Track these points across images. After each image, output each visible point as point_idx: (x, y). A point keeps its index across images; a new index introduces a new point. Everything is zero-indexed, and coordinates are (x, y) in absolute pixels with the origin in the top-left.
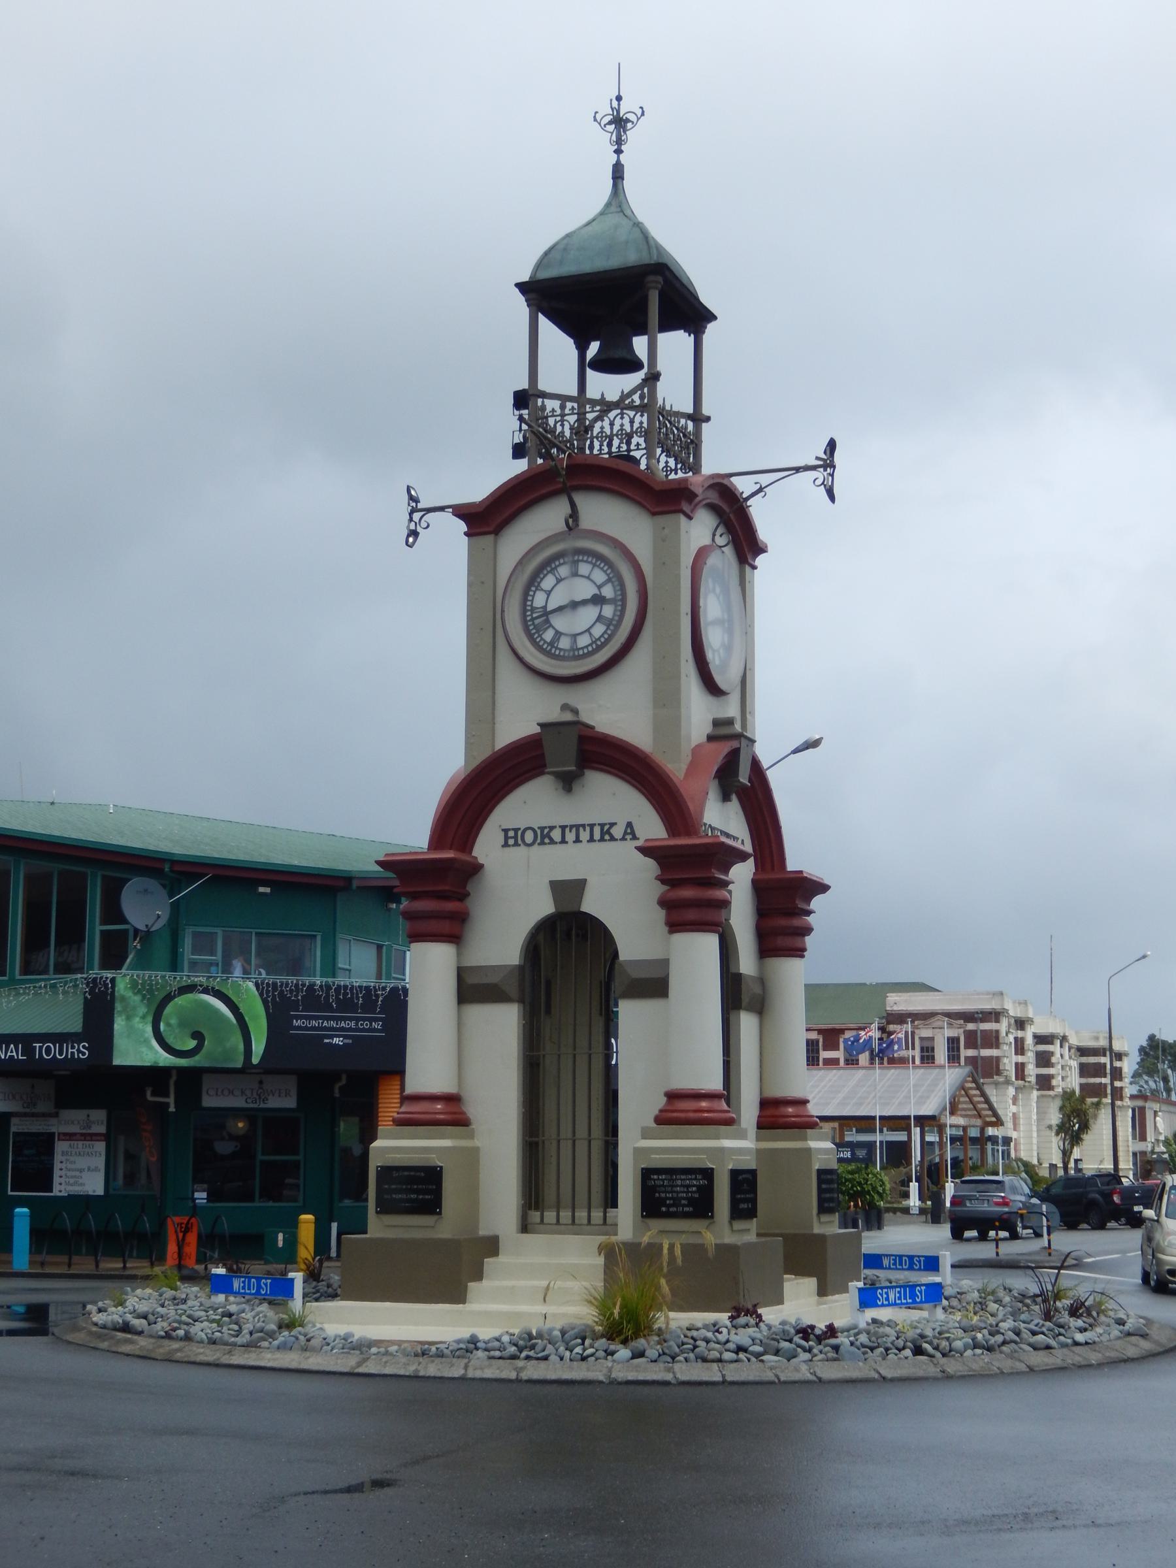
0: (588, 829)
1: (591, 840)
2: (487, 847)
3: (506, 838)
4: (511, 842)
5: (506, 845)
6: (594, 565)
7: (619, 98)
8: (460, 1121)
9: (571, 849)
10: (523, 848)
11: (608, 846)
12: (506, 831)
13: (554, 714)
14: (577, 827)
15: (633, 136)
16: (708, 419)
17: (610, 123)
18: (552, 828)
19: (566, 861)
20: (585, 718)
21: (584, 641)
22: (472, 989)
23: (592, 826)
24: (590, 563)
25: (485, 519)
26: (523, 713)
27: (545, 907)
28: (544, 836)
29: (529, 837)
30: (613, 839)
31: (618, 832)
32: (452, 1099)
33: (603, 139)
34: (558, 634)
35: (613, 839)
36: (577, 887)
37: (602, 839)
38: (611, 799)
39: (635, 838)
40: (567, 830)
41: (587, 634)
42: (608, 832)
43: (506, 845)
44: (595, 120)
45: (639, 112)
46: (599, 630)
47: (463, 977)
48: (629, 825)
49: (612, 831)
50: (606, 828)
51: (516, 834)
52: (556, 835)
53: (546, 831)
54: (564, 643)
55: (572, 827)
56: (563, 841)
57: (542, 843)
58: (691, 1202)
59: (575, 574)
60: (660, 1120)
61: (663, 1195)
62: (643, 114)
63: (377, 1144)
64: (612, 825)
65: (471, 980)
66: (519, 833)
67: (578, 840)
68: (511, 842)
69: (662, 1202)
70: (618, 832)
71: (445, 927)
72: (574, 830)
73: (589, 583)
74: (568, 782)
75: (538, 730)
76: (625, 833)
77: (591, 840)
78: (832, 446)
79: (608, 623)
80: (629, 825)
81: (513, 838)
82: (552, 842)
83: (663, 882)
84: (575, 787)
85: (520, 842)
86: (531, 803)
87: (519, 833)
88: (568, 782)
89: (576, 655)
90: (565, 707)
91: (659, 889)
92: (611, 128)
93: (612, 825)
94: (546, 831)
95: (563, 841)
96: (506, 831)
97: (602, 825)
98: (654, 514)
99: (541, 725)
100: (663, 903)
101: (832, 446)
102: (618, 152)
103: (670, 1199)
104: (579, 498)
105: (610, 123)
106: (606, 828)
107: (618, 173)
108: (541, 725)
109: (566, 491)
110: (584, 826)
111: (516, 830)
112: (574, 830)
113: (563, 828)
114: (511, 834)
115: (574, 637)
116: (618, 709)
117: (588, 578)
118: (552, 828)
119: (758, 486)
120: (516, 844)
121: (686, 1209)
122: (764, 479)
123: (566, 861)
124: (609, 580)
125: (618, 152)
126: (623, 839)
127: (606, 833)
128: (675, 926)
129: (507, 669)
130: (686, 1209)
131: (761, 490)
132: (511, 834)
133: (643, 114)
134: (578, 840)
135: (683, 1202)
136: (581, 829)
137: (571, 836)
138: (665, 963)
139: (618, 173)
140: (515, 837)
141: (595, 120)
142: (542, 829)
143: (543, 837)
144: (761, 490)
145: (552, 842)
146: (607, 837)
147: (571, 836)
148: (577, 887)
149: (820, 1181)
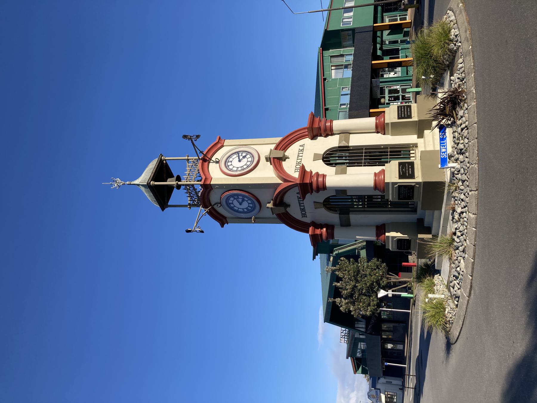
2: (307, 220)
28: (303, 210)
52: (302, 207)
54: (251, 205)
59: (232, 203)
63: (390, 249)
78: (185, 137)
81: (304, 215)
86: (295, 212)
89: (253, 203)
101: (185, 137)
115: (249, 204)
122: (198, 152)
137: (302, 205)
147: (302, 205)
149: (402, 118)
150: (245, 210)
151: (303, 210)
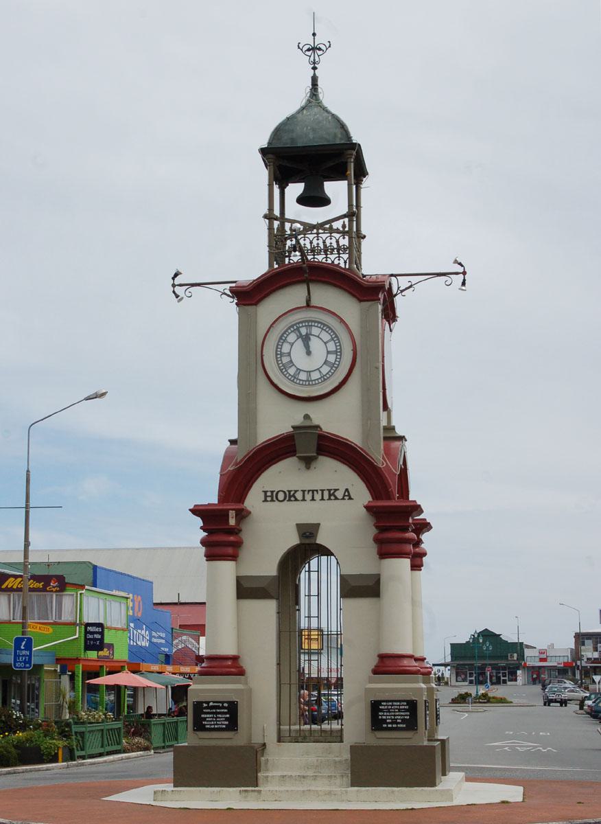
0: (320, 492)
1: (322, 499)
2: (253, 500)
3: (266, 496)
4: (269, 499)
5: (265, 500)
6: (322, 329)
7: (314, 34)
8: (241, 673)
9: (308, 504)
10: (277, 502)
11: (333, 503)
12: (265, 492)
13: (298, 420)
14: (313, 491)
15: (325, 61)
16: (364, 237)
17: (309, 50)
18: (296, 491)
19: (306, 512)
20: (316, 422)
21: (315, 376)
22: (247, 590)
23: (322, 491)
24: (320, 327)
25: (248, 296)
26: (277, 420)
27: (294, 540)
28: (290, 496)
29: (281, 496)
30: (336, 498)
31: (339, 494)
32: (235, 658)
33: (304, 61)
34: (299, 370)
35: (336, 498)
37: (329, 499)
39: (350, 498)
40: (306, 493)
41: (318, 371)
42: (333, 494)
43: (265, 500)
44: (299, 48)
45: (328, 45)
46: (325, 370)
47: (239, 581)
48: (347, 490)
49: (336, 494)
50: (332, 492)
51: (272, 494)
52: (299, 495)
53: (292, 493)
54: (303, 376)
55: (309, 491)
56: (304, 500)
57: (289, 500)
58: (404, 721)
60: (375, 672)
61: (384, 717)
62: (330, 46)
64: (336, 490)
65: (246, 585)
66: (275, 493)
67: (313, 499)
68: (269, 499)
69: (384, 721)
70: (339, 494)
71: (230, 550)
72: (311, 492)
73: (317, 338)
74: (308, 462)
75: (292, 430)
76: (344, 495)
77: (322, 499)
79: (332, 365)
80: (347, 490)
81: (270, 497)
82: (296, 500)
83: (377, 527)
84: (312, 467)
85: (275, 499)
87: (275, 493)
88: (308, 462)
90: (307, 417)
91: (374, 531)
92: (309, 53)
93: (336, 490)
94: (292, 493)
95: (304, 500)
96: (265, 492)
97: (329, 490)
98: (360, 301)
99: (293, 427)
100: (377, 540)
102: (314, 68)
103: (389, 719)
104: (313, 287)
105: (309, 50)
106: (332, 492)
107: (314, 80)
108: (293, 427)
109: (307, 282)
110: (317, 491)
111: (272, 492)
112: (311, 492)
113: (304, 491)
114: (269, 494)
116: (340, 419)
117: (318, 337)
118: (296, 491)
119: (410, 284)
120: (272, 500)
121: (401, 726)
122: (414, 279)
123: (306, 512)
124: (332, 339)
125: (314, 68)
126: (343, 499)
127: (332, 494)
128: (383, 555)
129: (264, 390)
130: (401, 726)
131: (411, 286)
132: (269, 494)
133: (330, 46)
134: (313, 499)
135: (398, 721)
136: (315, 492)
137: (308, 497)
138: (379, 575)
139: (314, 80)
140: (272, 496)
141: (299, 48)
142: (290, 491)
143: (290, 497)
144: (411, 286)
145: (296, 500)
146: (332, 498)
147: (308, 497)
150: (285, 360)
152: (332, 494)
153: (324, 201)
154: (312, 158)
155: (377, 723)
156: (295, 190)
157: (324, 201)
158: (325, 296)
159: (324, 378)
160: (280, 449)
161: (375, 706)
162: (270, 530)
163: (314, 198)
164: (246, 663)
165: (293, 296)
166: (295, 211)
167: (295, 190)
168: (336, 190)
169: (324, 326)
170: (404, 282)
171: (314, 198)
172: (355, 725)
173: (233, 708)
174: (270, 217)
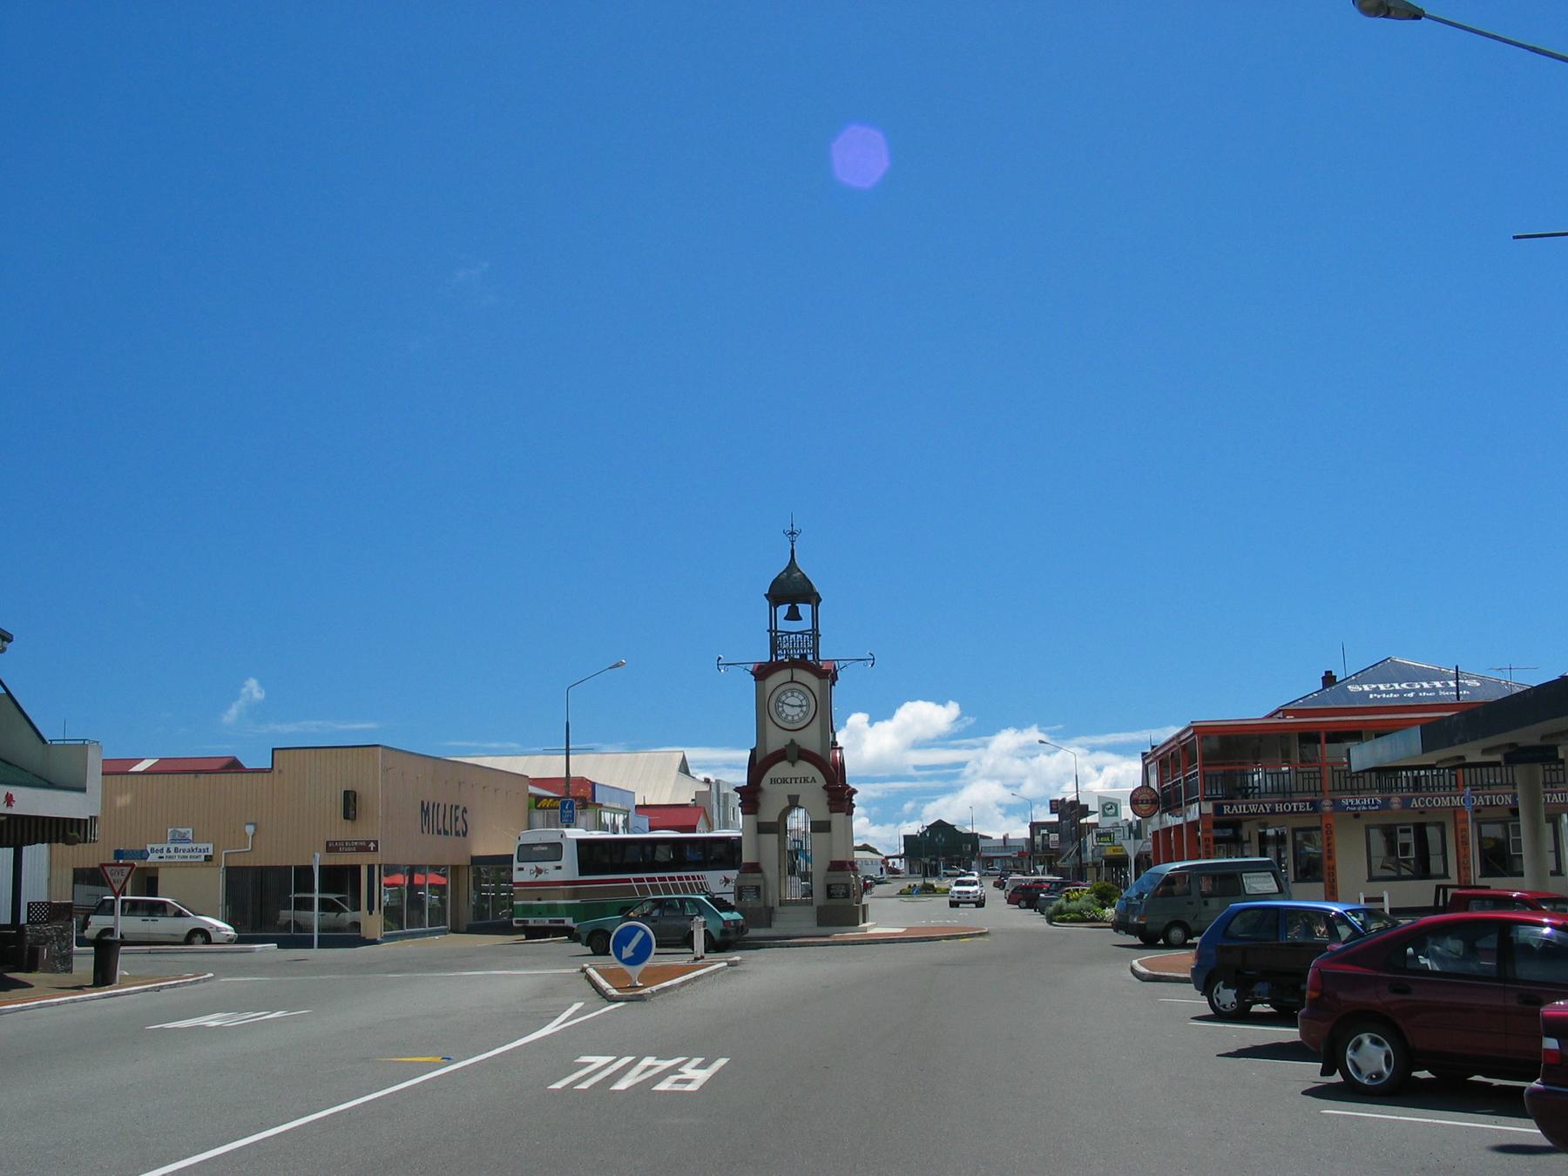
2: (765, 783)
19: (793, 789)
20: (798, 741)
28: (784, 781)
33: (787, 540)
36: (797, 797)
38: (806, 769)
81: (774, 781)
86: (781, 769)
116: (810, 740)
123: (793, 789)
127: (806, 780)
128: (832, 811)
148: (797, 797)
151: (784, 781)
152: (806, 780)
153: (799, 618)
154: (792, 591)
155: (830, 895)
156: (783, 610)
157: (799, 618)
158: (802, 675)
159: (801, 720)
160: (779, 756)
161: (829, 887)
162: (773, 798)
163: (793, 615)
164: (763, 866)
165: (784, 675)
166: (784, 625)
167: (783, 610)
168: (805, 609)
169: (800, 692)
170: (842, 664)
171: (793, 615)
172: (819, 897)
173: (758, 888)
174: (770, 631)
